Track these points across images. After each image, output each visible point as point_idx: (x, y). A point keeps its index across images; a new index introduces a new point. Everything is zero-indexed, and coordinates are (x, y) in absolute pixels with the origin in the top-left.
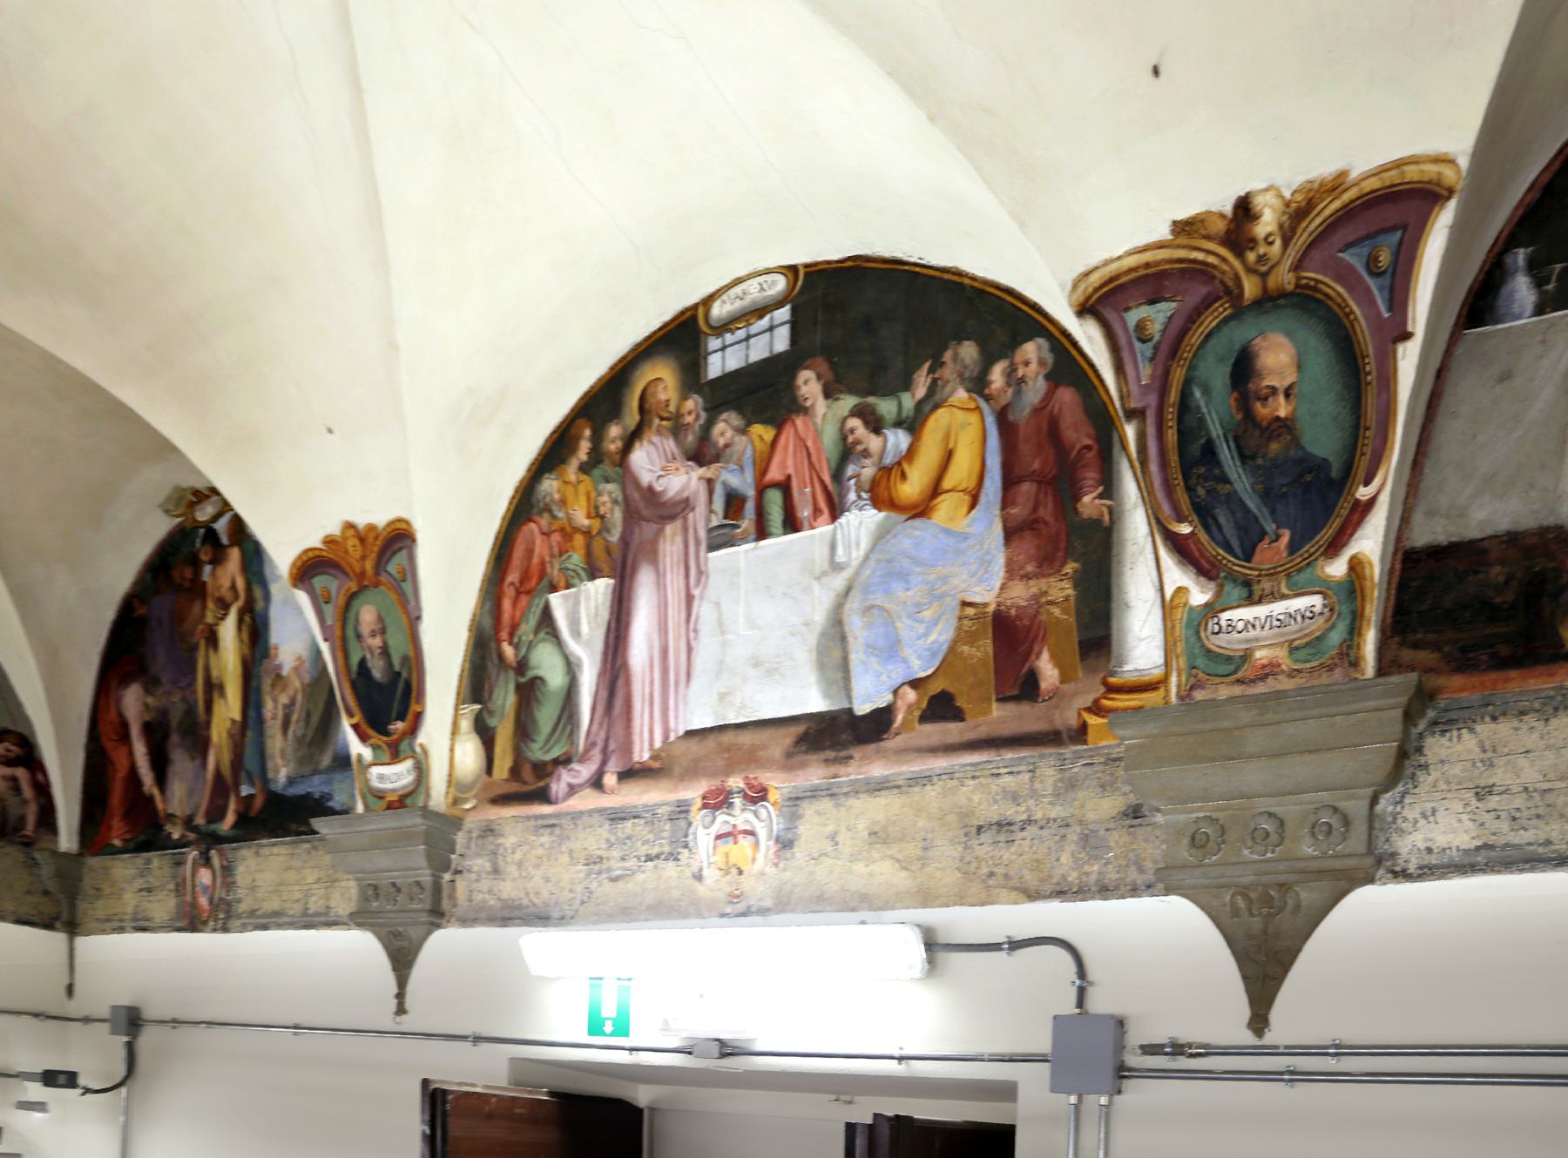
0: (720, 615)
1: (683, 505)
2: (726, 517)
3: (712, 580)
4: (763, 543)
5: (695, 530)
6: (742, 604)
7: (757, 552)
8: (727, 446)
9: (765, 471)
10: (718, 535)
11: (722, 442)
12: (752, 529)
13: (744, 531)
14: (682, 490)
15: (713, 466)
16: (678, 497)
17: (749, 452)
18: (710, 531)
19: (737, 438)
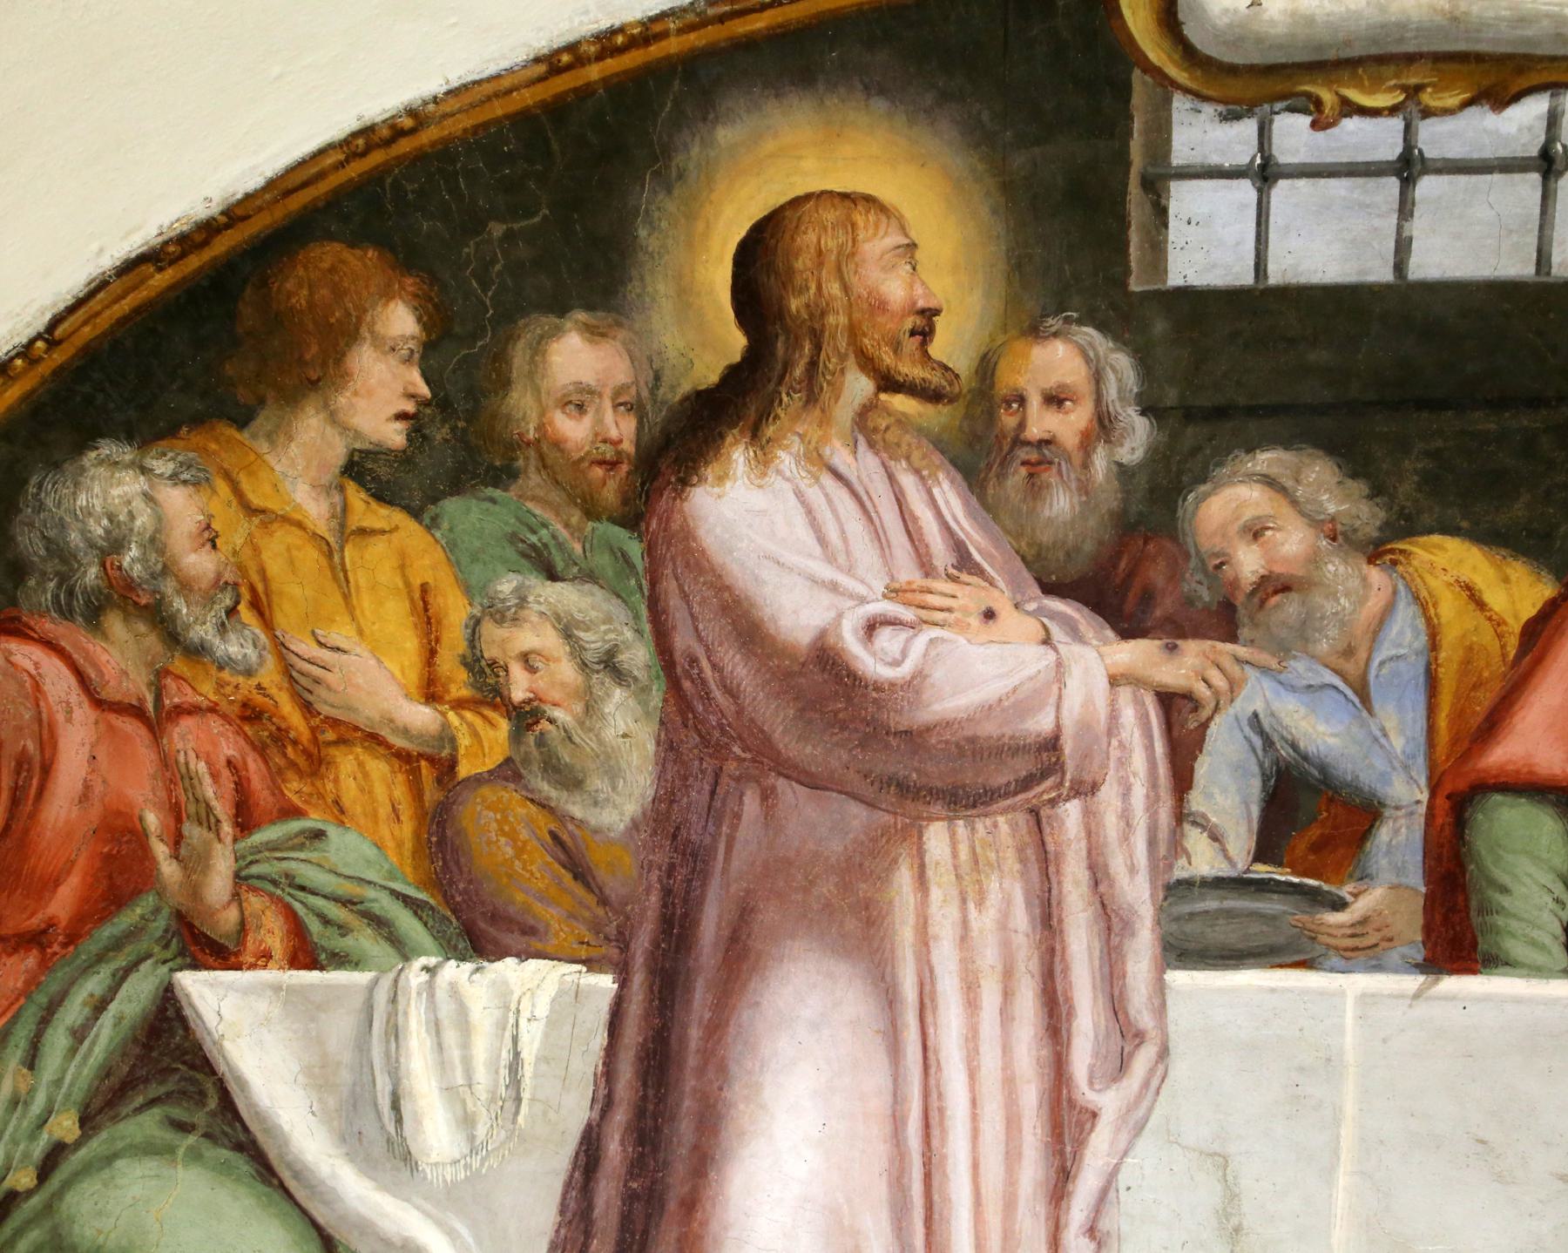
0: (1232, 1196)
1: (1023, 766)
2: (1263, 853)
3: (1181, 1068)
4: (1451, 984)
5: (1098, 874)
6: (1342, 1180)
7: (1422, 1010)
8: (1274, 586)
9: (1493, 724)
10: (1229, 914)
11: (1249, 563)
12: (1409, 922)
13: (1364, 921)
14: (1019, 703)
15: (1193, 650)
16: (989, 729)
17: (1404, 633)
18: (1178, 890)
19: (1336, 568)
